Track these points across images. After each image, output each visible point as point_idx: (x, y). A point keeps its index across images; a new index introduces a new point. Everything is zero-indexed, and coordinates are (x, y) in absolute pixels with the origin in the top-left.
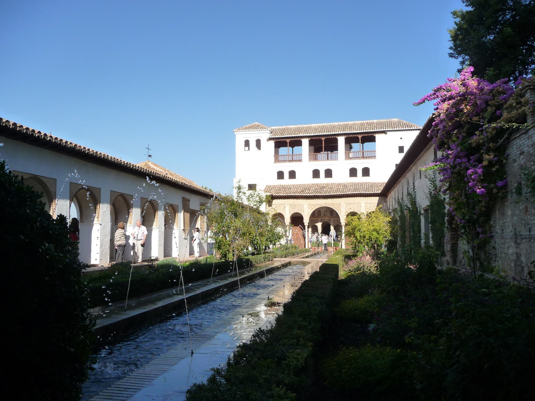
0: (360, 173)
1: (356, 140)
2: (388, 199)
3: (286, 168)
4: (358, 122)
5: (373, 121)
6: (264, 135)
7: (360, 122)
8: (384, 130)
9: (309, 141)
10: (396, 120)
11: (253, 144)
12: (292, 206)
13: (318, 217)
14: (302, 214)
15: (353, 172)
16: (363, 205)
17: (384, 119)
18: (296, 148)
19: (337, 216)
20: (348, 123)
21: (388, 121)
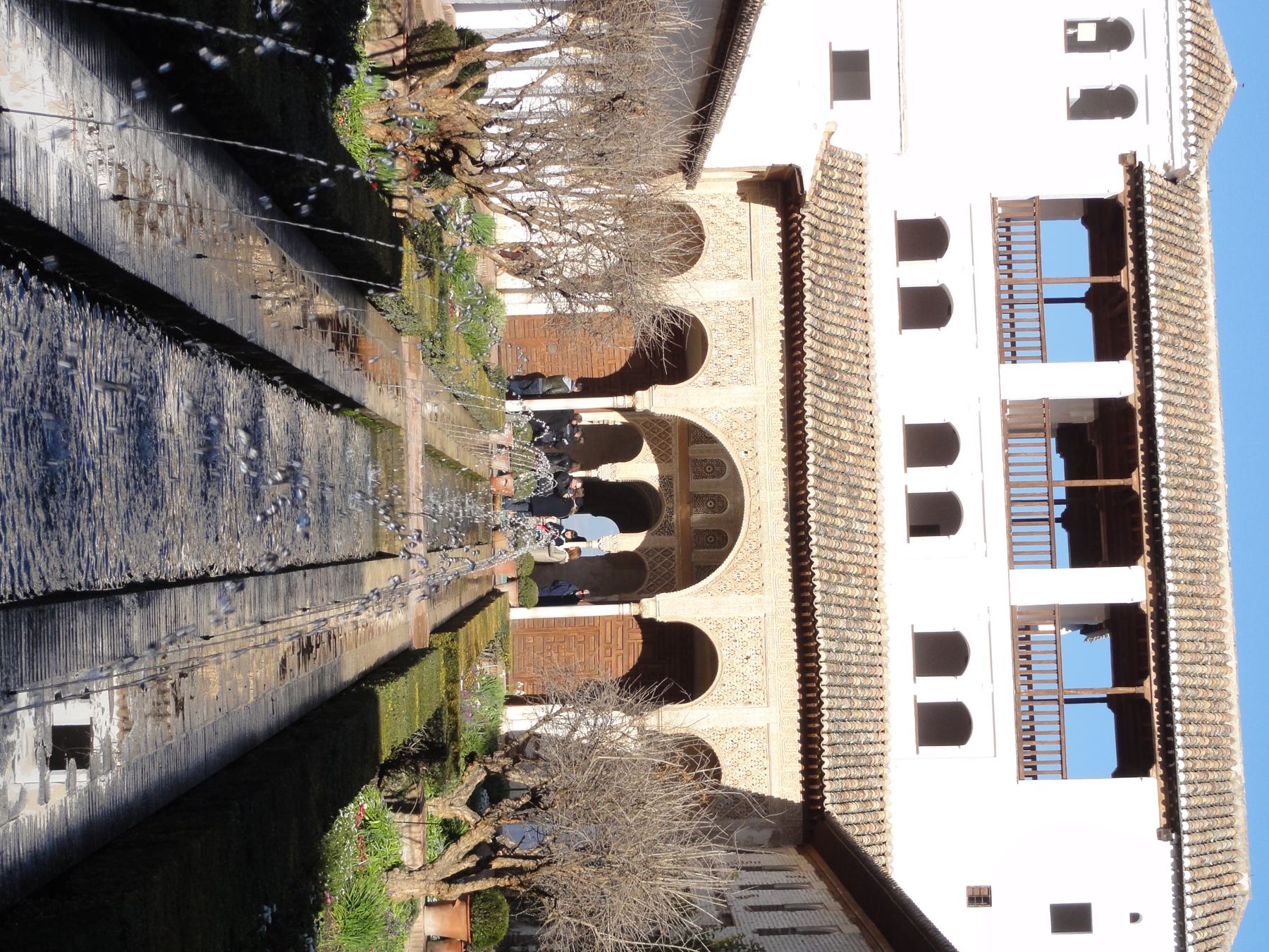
0: (940, 690)
1: (1129, 664)
2: (790, 856)
3: (966, 271)
4: (1233, 676)
5: (1238, 757)
6: (1155, 136)
7: (1233, 688)
8: (1185, 826)
9: (1123, 401)
10: (1245, 882)
11: (1105, 71)
12: (745, 311)
13: (685, 459)
14: (699, 378)
15: (942, 653)
16: (756, 716)
17: (1250, 818)
18: (1083, 318)
19: (695, 572)
20: (1229, 619)
21: (1240, 844)
